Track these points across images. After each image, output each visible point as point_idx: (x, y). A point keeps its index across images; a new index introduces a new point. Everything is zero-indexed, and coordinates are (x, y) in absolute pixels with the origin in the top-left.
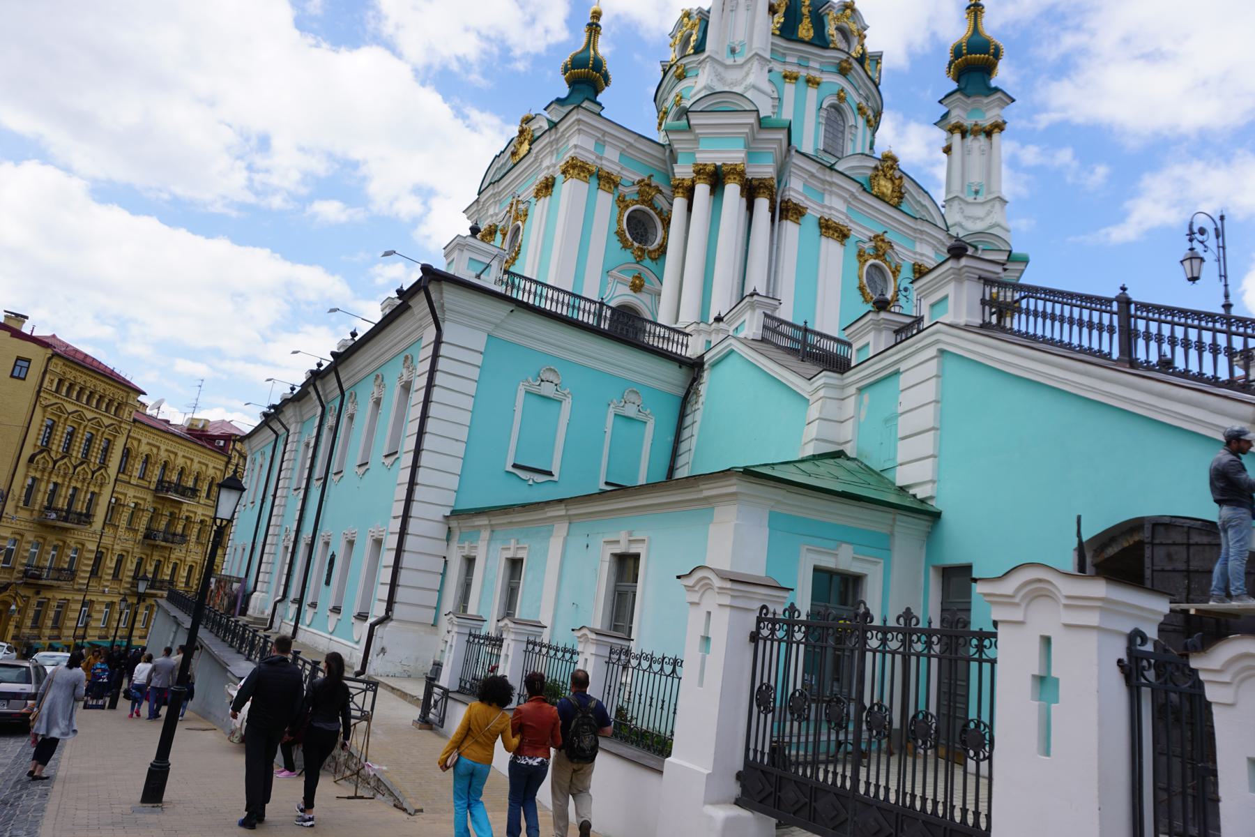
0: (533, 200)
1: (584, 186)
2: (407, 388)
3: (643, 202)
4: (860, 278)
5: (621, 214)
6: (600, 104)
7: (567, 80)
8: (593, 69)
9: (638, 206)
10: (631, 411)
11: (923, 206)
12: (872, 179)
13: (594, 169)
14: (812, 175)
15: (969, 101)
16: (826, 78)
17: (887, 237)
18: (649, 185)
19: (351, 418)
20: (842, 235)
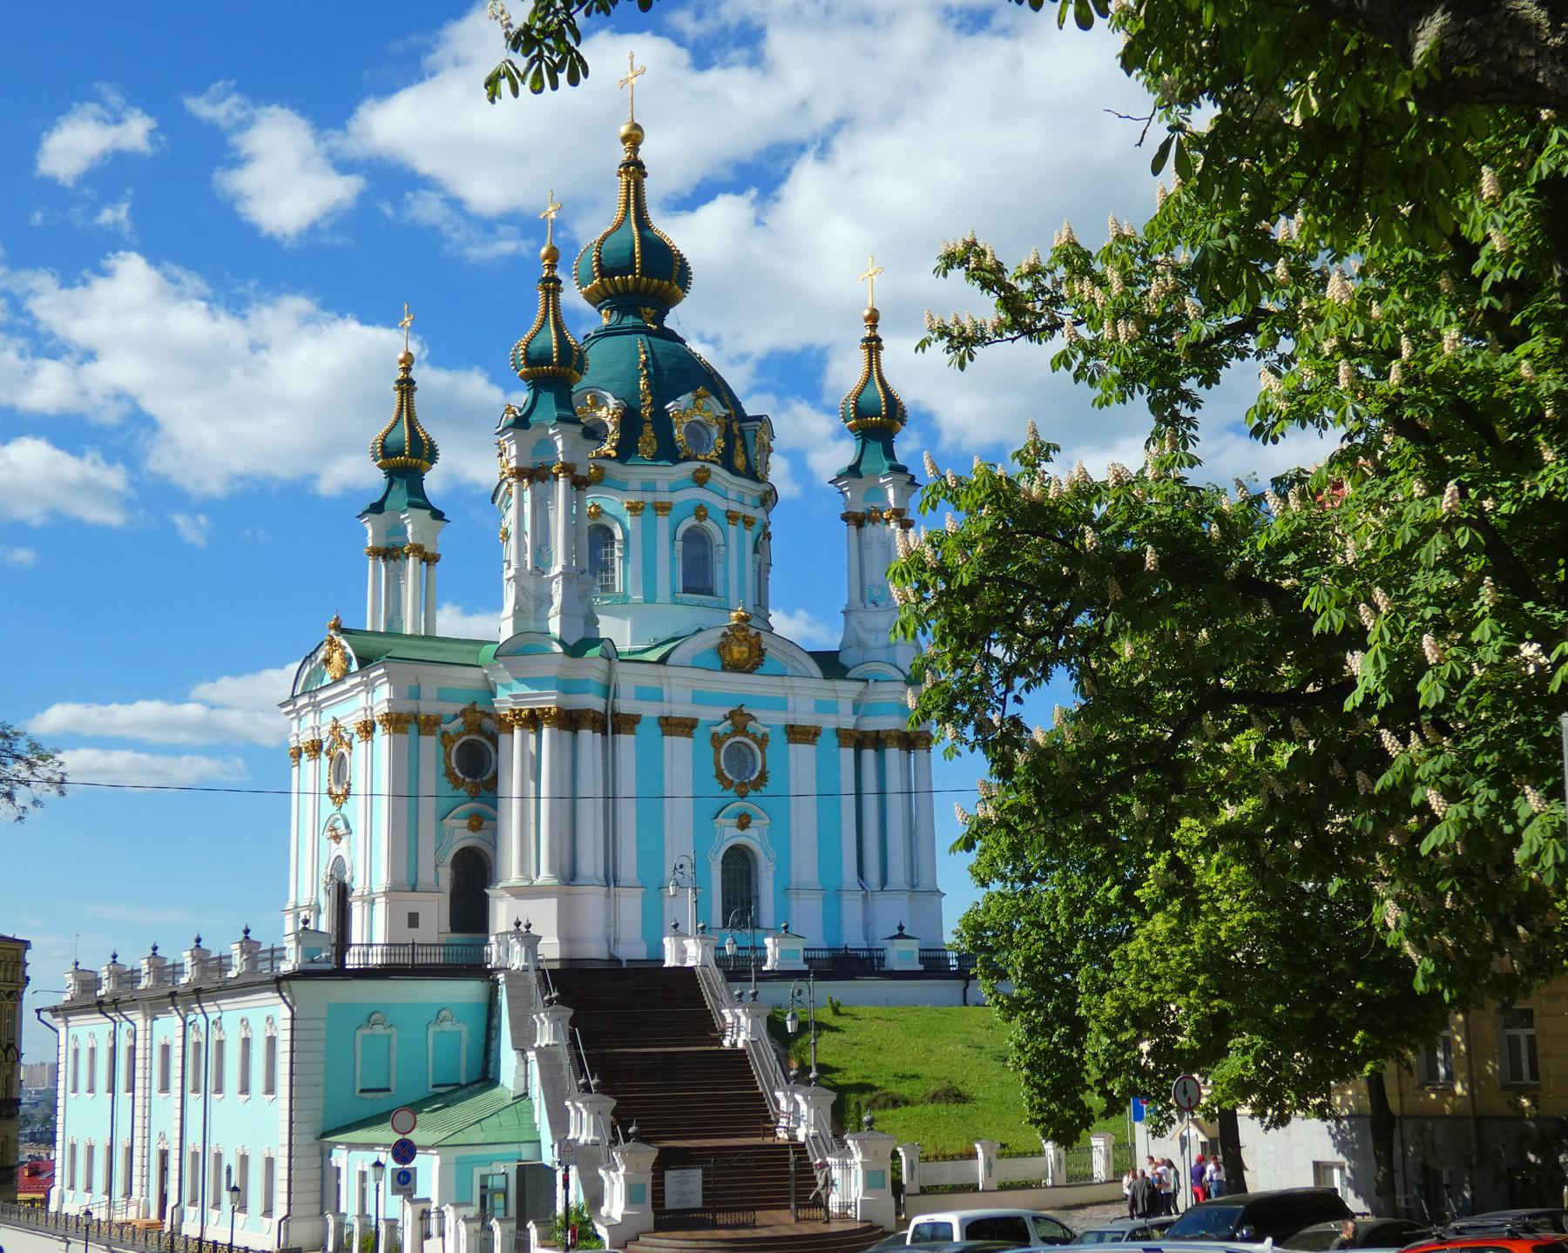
0: (357, 738)
2: (271, 1041)
3: (469, 732)
4: (717, 764)
5: (448, 755)
7: (380, 466)
8: (411, 456)
9: (465, 738)
10: (447, 1026)
12: (722, 648)
16: (677, 498)
17: (745, 711)
19: (220, 1044)
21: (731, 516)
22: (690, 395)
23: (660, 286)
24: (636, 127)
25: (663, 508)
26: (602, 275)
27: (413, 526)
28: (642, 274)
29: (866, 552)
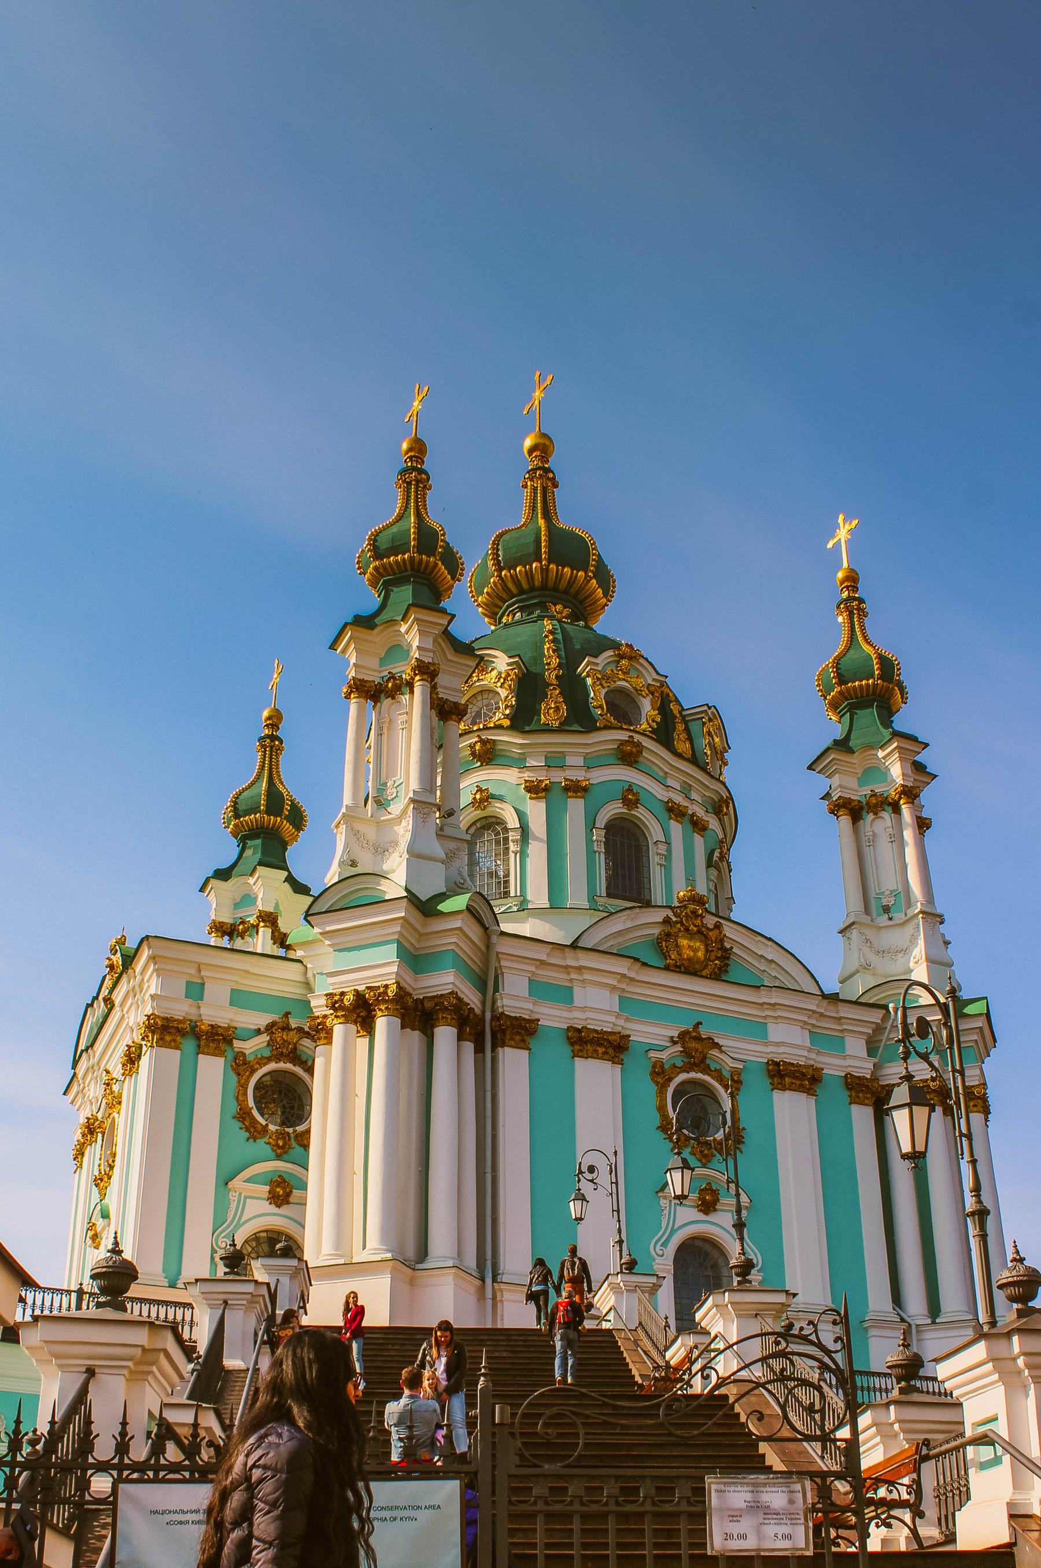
1: (173, 1056)
3: (278, 1057)
4: (662, 1109)
6: (285, 868)
9: (272, 1066)
11: (772, 961)
12: (664, 942)
13: (187, 1025)
14: (543, 963)
15: (854, 759)
16: (598, 776)
17: (704, 1031)
18: (287, 1028)
20: (611, 1047)
21: (674, 811)
22: (610, 653)
23: (573, 579)
24: (544, 436)
25: (575, 789)
26: (500, 570)
27: (266, 888)
28: (550, 561)
29: (868, 852)
